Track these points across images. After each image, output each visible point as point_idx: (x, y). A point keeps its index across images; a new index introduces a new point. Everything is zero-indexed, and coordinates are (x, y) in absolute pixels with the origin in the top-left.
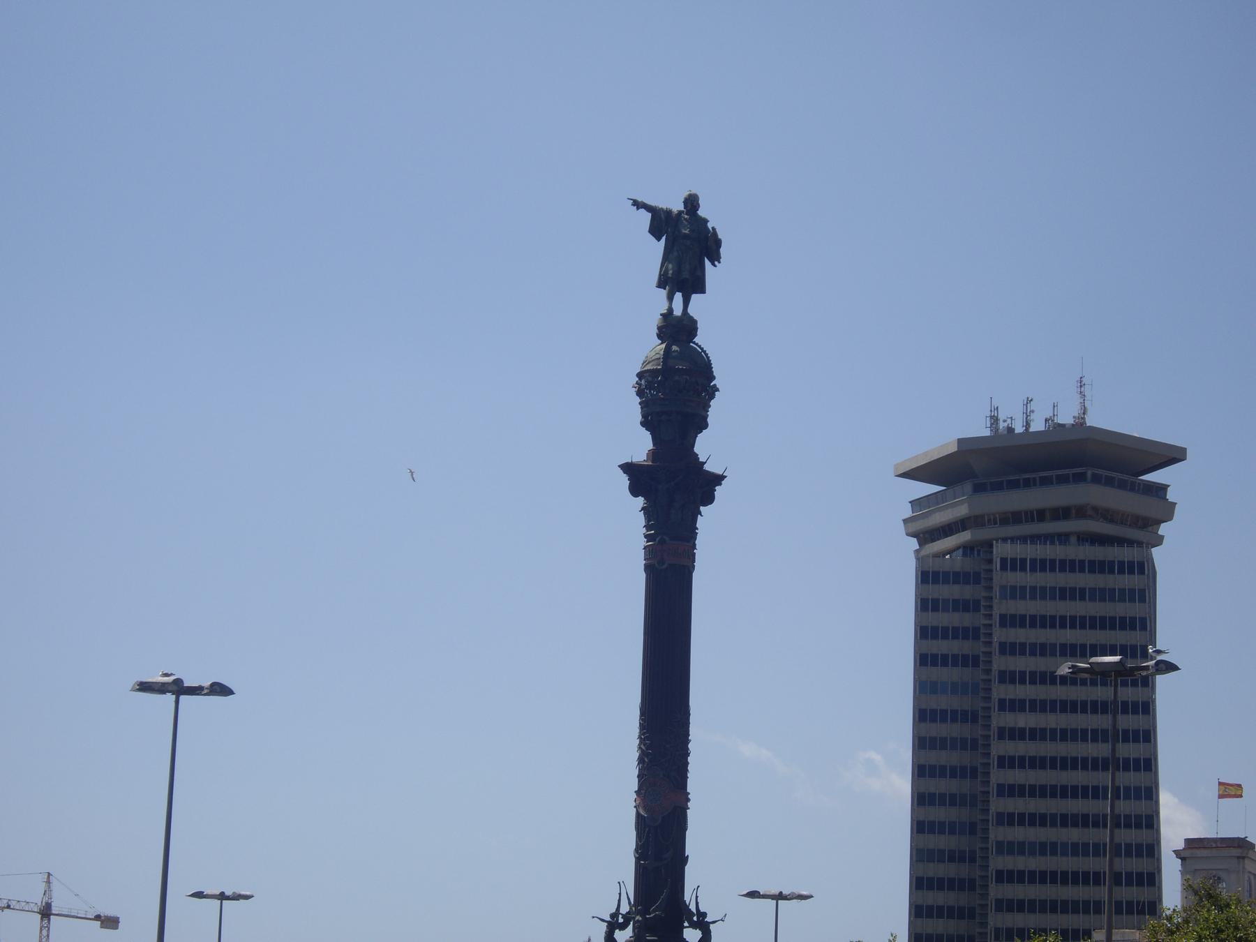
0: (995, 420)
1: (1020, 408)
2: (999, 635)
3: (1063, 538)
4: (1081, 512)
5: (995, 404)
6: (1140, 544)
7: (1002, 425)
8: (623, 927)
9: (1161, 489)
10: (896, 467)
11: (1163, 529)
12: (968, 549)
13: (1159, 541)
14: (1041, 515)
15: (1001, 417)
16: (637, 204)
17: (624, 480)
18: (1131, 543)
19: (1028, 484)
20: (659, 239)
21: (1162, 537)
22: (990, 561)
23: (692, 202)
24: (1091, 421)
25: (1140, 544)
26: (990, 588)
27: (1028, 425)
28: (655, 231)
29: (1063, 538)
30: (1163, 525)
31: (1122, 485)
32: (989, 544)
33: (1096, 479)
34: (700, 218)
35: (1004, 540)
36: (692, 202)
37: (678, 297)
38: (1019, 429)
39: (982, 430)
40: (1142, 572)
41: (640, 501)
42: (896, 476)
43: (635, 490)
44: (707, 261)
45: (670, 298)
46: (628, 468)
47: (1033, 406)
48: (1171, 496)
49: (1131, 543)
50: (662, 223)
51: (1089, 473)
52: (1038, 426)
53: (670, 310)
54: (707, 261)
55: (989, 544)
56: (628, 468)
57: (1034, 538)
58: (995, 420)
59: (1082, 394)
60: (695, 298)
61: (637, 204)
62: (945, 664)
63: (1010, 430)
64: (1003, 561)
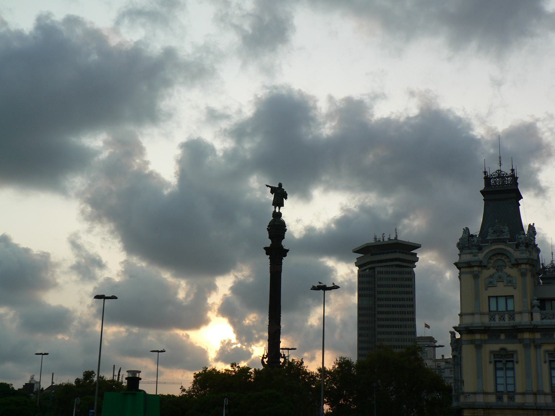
0: (376, 239)
1: (382, 236)
3: (392, 266)
5: (376, 235)
6: (410, 267)
7: (378, 240)
8: (266, 358)
10: (353, 250)
11: (416, 264)
12: (370, 269)
13: (415, 267)
14: (386, 261)
15: (377, 237)
16: (267, 186)
17: (265, 251)
18: (408, 267)
19: (383, 254)
20: (273, 194)
21: (416, 266)
23: (280, 185)
24: (399, 238)
25: (410, 267)
26: (375, 278)
27: (383, 240)
28: (272, 192)
29: (392, 266)
31: (406, 253)
32: (374, 268)
33: (399, 252)
34: (519, 203)
35: (378, 267)
36: (280, 185)
37: (277, 208)
38: (382, 241)
40: (411, 274)
41: (269, 256)
42: (354, 252)
43: (267, 254)
44: (284, 199)
45: (275, 208)
46: (265, 248)
47: (384, 235)
49: (408, 267)
50: (273, 190)
52: (386, 239)
53: (275, 211)
54: (284, 199)
55: (374, 268)
56: (265, 248)
57: (385, 266)
58: (376, 239)
59: (396, 232)
60: (281, 208)
61: (267, 186)
62: (365, 296)
63: (380, 241)
64: (378, 272)
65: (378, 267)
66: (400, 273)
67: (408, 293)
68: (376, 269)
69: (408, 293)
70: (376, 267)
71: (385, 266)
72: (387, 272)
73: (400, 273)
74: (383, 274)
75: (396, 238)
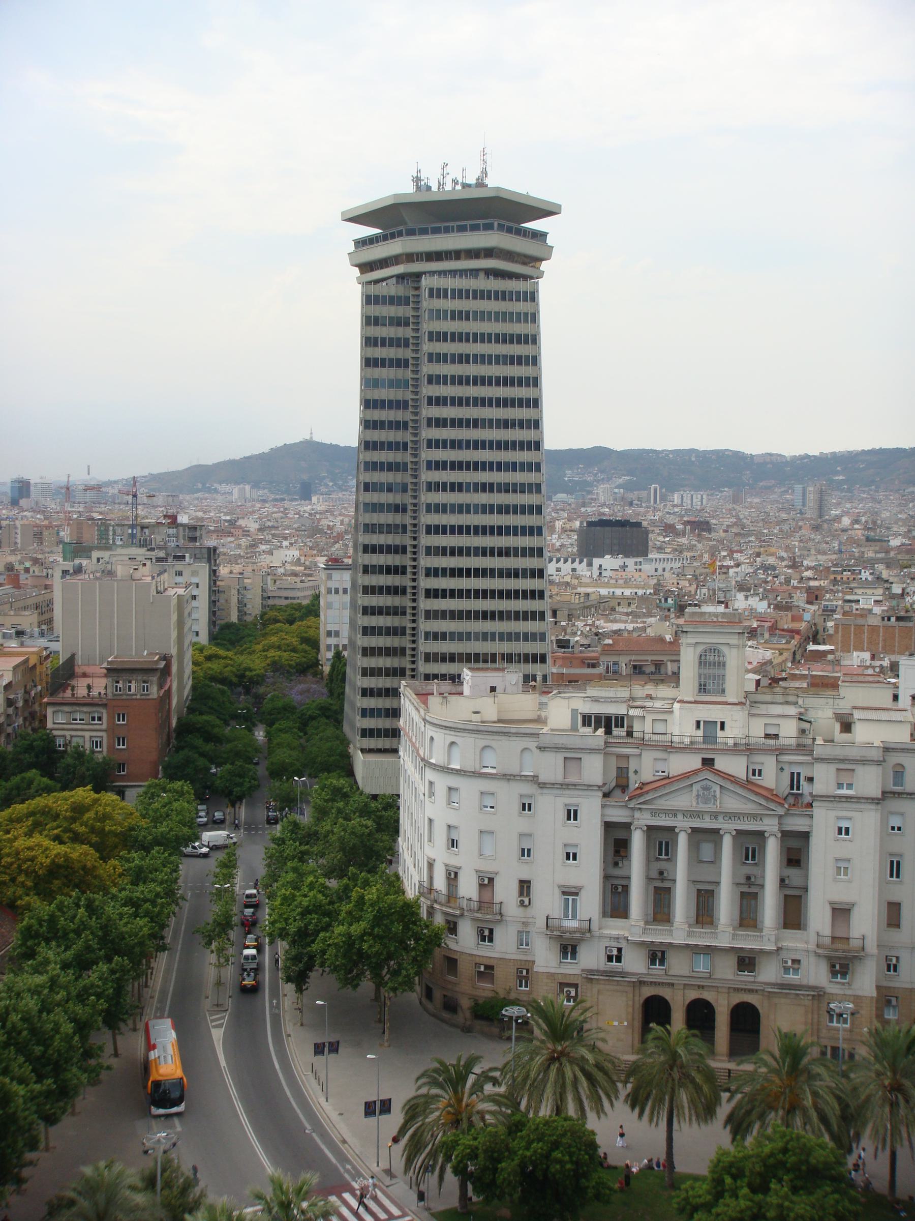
1: (439, 171)
2: (427, 347)
3: (474, 273)
4: (489, 253)
9: (540, 236)
10: (342, 213)
11: (544, 266)
12: (400, 277)
13: (540, 275)
14: (457, 255)
19: (447, 230)
22: (417, 288)
29: (474, 273)
30: (544, 262)
31: (509, 230)
32: (418, 276)
35: (432, 273)
38: (435, 188)
39: (406, 188)
47: (448, 170)
48: (549, 241)
51: (496, 224)
52: (448, 187)
57: (453, 273)
58: (417, 180)
59: (485, 162)
63: (429, 188)
65: (432, 273)
66: (502, 296)
67: (520, 360)
68: (425, 282)
69: (520, 360)
70: (425, 273)
71: (453, 273)
72: (461, 291)
73: (502, 296)
74: (446, 296)
75: (480, 184)
